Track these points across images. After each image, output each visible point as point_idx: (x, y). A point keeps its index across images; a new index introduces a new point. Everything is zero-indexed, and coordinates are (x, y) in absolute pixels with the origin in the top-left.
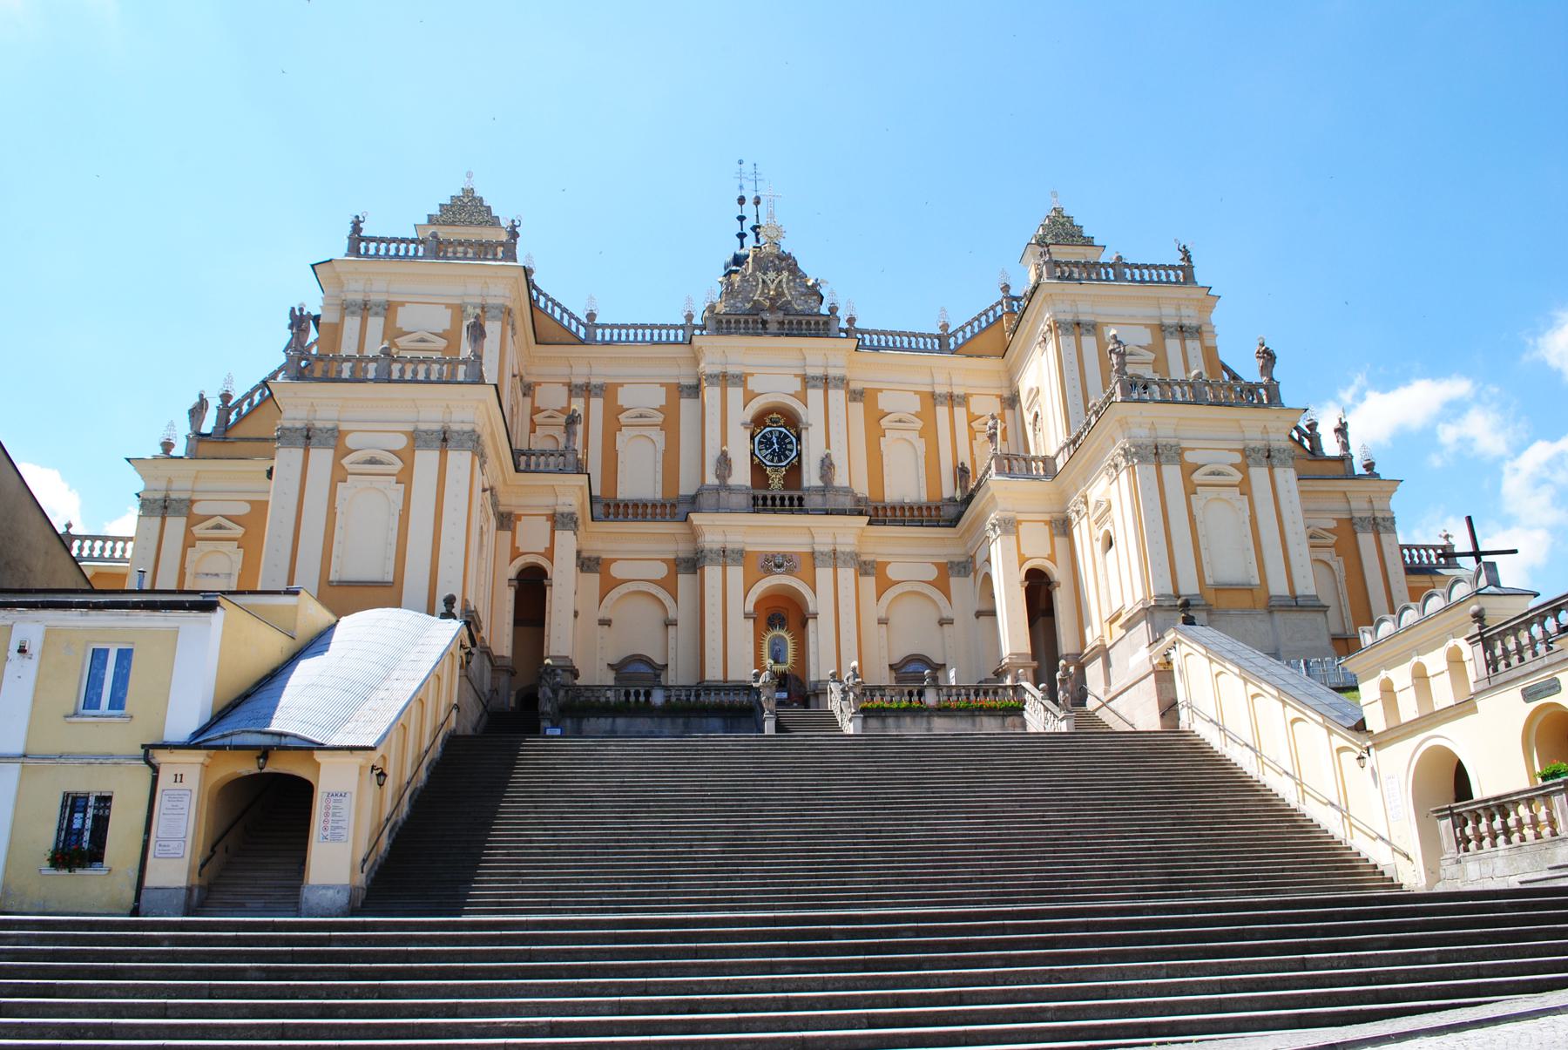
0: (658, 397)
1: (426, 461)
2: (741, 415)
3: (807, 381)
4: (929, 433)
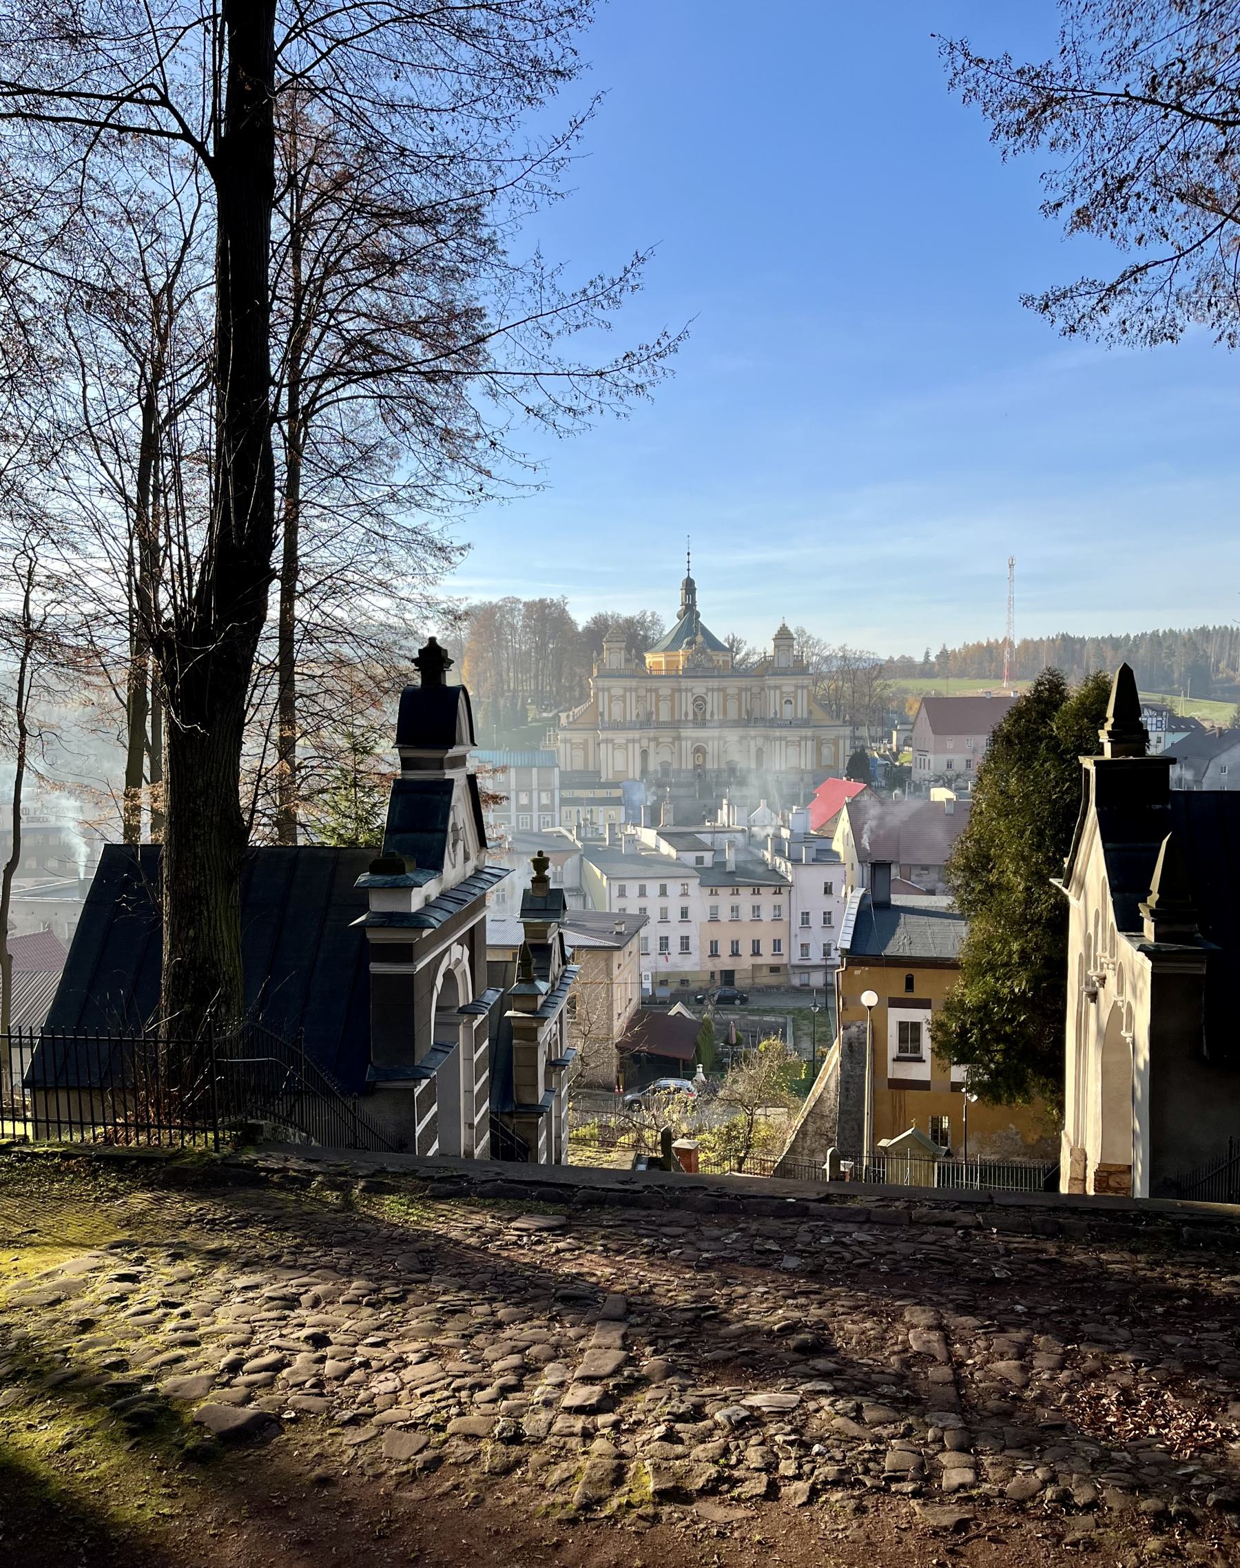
0: (669, 692)
1: (630, 746)
2: (690, 700)
3: (708, 689)
4: (740, 700)
